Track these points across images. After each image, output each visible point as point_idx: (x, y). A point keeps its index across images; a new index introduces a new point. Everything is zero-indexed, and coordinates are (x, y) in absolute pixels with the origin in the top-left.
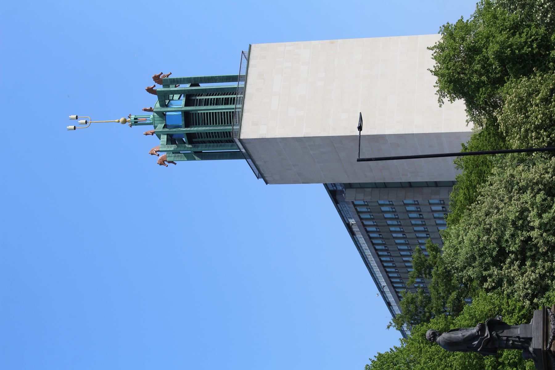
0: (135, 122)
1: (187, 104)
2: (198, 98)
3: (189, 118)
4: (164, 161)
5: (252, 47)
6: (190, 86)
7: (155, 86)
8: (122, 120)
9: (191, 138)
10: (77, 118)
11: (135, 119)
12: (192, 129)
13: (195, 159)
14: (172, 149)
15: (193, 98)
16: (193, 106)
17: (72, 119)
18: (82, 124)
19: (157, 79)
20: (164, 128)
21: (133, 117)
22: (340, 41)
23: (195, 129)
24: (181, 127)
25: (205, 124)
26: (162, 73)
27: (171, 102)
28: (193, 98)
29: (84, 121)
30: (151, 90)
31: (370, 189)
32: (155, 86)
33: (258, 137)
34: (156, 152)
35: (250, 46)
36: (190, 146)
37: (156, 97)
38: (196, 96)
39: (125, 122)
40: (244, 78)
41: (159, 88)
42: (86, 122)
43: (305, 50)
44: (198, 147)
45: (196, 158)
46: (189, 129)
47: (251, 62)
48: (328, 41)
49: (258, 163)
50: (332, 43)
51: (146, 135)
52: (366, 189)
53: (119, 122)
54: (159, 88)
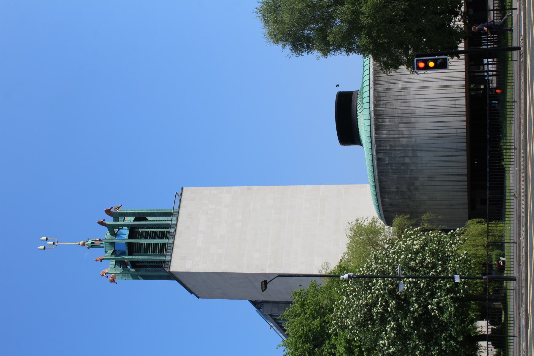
0: (92, 246)
1: (130, 237)
2: (140, 230)
3: (132, 249)
4: (114, 280)
5: (184, 189)
6: (134, 221)
7: (104, 220)
8: (81, 243)
9: (134, 264)
10: (47, 239)
11: (92, 243)
12: (134, 257)
13: (139, 279)
14: (119, 272)
15: (136, 230)
16: (136, 238)
17: (43, 240)
18: (50, 245)
19: (108, 212)
20: (112, 255)
21: (90, 241)
22: (256, 188)
23: (136, 257)
24: (125, 255)
25: (145, 253)
26: (112, 208)
27: (121, 230)
28: (136, 230)
29: (52, 243)
30: (102, 223)
31: (283, 305)
32: (104, 220)
33: (184, 271)
34: (106, 274)
35: (182, 188)
36: (133, 270)
37: (106, 228)
38: (139, 228)
39: (84, 245)
40: (177, 214)
41: (110, 220)
42: (54, 243)
43: (226, 195)
44: (139, 271)
45: (140, 278)
46: (131, 257)
47: (182, 204)
48: (246, 187)
49: (188, 286)
50: (249, 189)
51: (97, 261)
52: (280, 305)
53: (79, 244)
54: (110, 220)
